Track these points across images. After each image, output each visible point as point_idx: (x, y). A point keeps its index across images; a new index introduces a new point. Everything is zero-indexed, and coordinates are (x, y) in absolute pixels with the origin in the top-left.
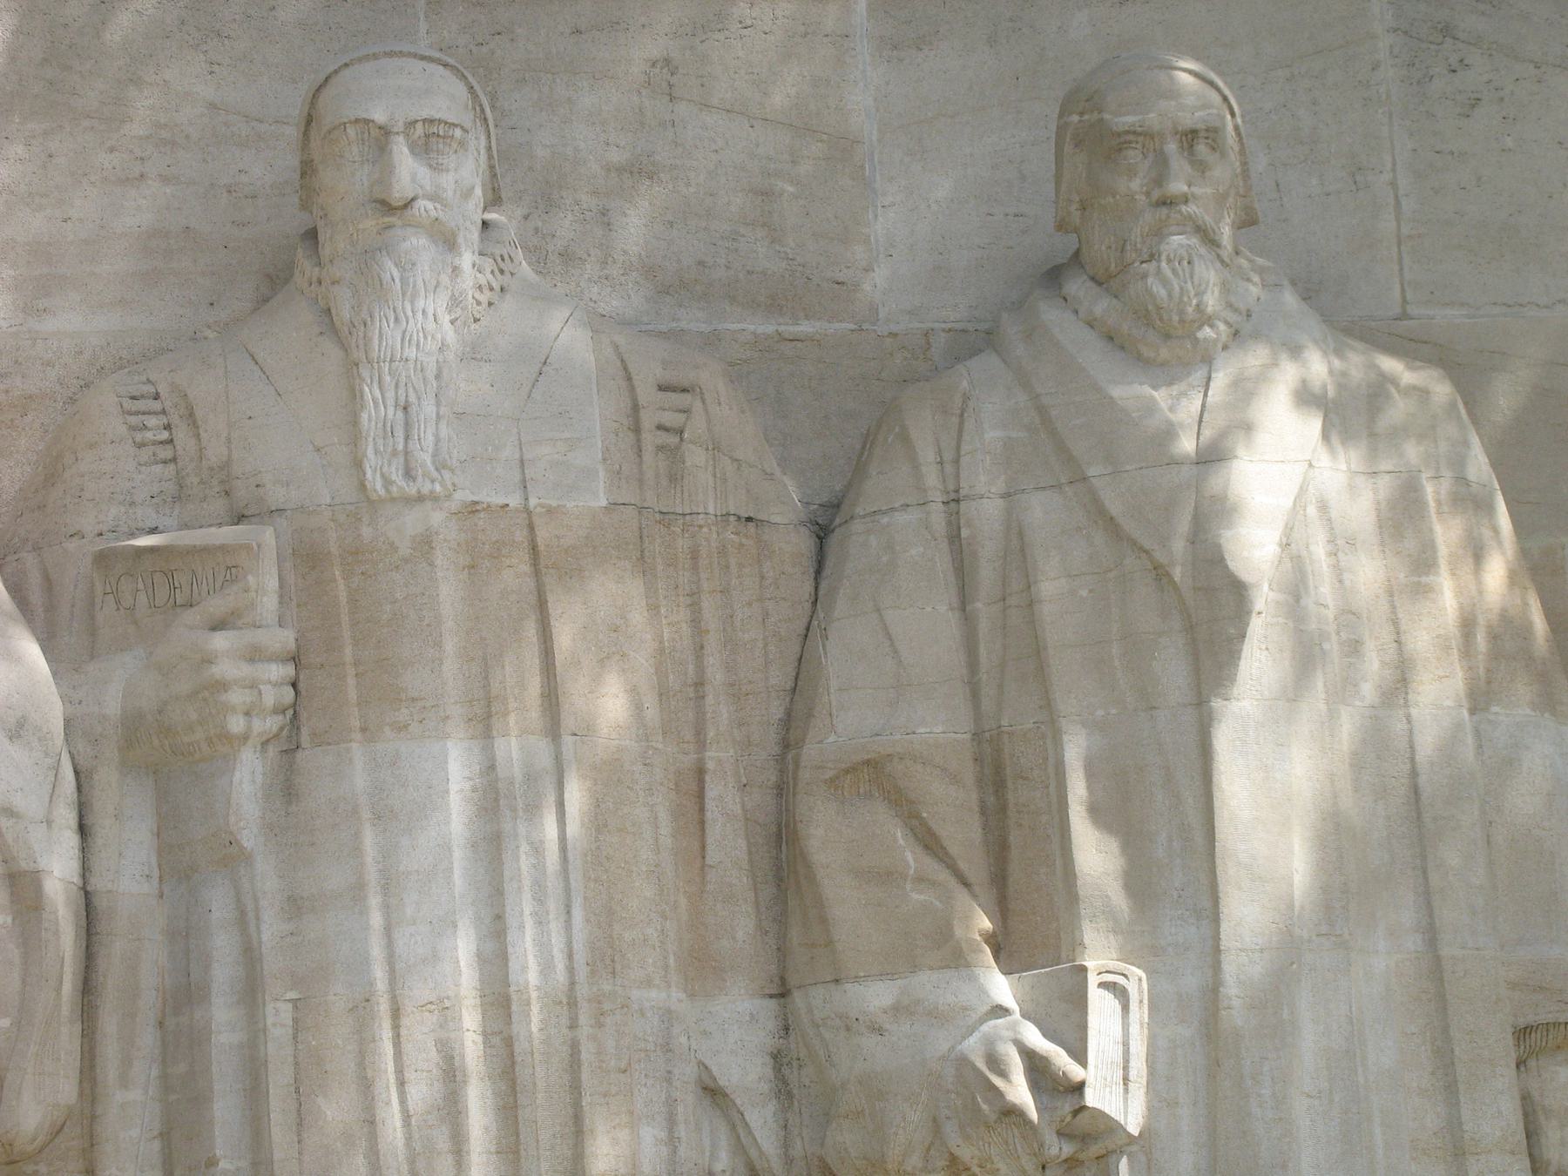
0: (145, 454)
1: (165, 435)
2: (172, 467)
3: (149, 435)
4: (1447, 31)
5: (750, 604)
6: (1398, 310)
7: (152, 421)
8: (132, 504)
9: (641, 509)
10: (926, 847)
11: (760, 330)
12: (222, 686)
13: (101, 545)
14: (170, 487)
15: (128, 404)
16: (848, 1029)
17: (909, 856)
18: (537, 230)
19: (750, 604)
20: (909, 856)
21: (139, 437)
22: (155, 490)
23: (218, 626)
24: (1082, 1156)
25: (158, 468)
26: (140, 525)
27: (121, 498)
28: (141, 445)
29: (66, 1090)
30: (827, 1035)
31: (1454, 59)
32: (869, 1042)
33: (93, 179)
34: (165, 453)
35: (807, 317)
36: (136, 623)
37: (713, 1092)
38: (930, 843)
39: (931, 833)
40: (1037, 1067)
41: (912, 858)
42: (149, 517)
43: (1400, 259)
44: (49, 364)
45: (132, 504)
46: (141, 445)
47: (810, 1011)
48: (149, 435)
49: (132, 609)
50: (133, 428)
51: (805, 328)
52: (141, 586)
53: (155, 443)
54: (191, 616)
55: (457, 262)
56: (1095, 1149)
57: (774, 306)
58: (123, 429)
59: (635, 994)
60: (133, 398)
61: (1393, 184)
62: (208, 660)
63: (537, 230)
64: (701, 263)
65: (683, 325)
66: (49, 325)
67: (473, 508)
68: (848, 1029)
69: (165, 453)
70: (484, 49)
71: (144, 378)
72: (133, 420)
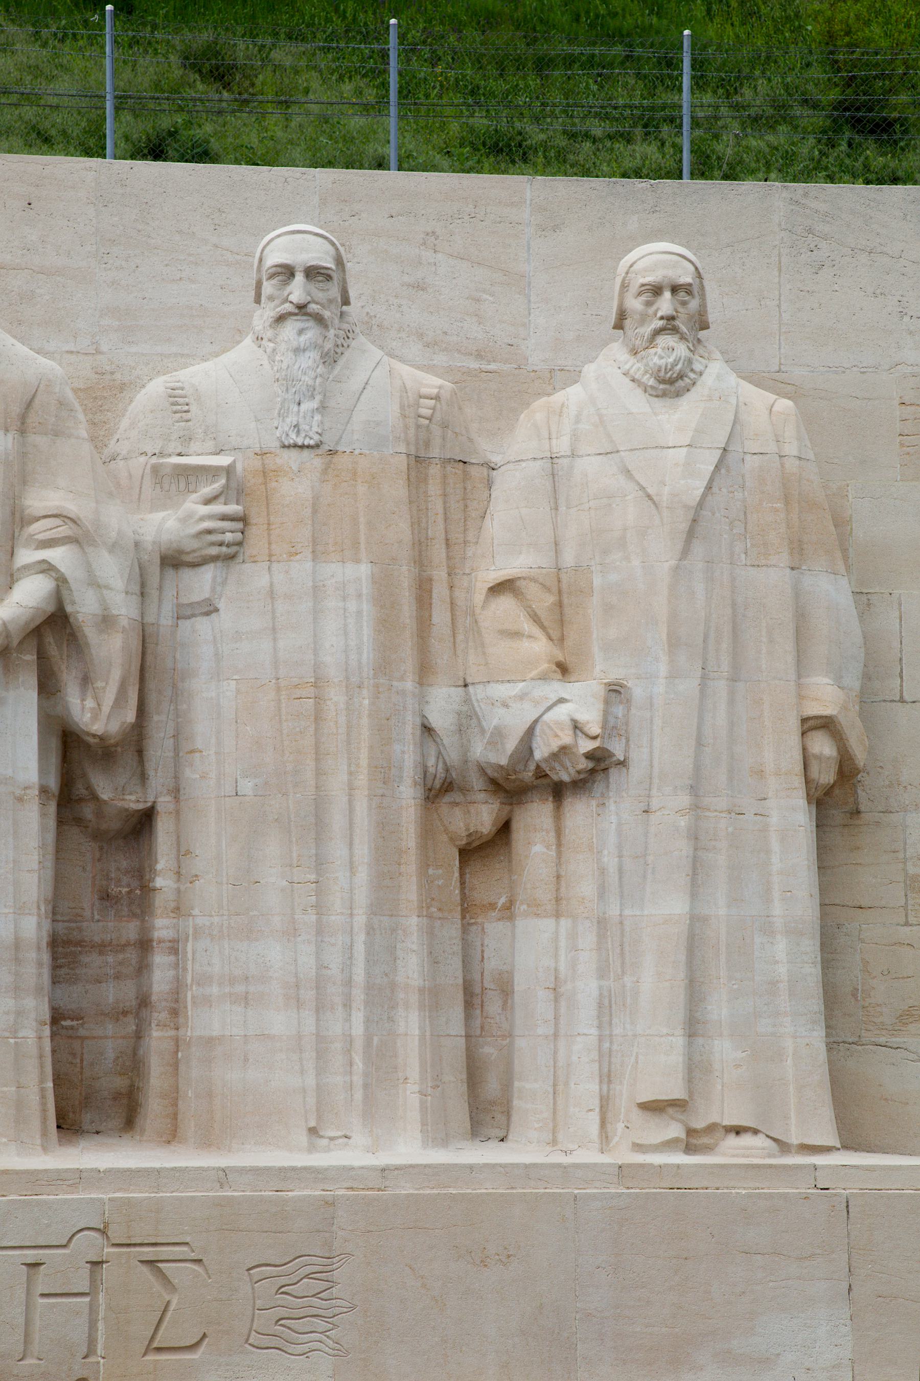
4: (810, 231)
5: (458, 502)
6: (777, 368)
9: (408, 455)
10: (534, 621)
11: (472, 366)
13: (154, 460)
16: (493, 704)
17: (526, 626)
18: (368, 313)
19: (458, 502)
20: (526, 626)
22: (181, 434)
23: (208, 502)
24: (598, 768)
29: (130, 716)
30: (483, 707)
31: (812, 246)
32: (502, 711)
35: (494, 361)
37: (427, 729)
38: (536, 619)
39: (536, 614)
40: (576, 727)
41: (527, 626)
43: (780, 343)
46: (175, 412)
47: (476, 695)
51: (492, 367)
54: (194, 496)
55: (327, 334)
56: (603, 766)
57: (479, 356)
59: (395, 683)
61: (779, 306)
63: (368, 313)
64: (445, 333)
65: (435, 362)
67: (332, 453)
68: (493, 704)
70: (347, 223)
72: (172, 399)
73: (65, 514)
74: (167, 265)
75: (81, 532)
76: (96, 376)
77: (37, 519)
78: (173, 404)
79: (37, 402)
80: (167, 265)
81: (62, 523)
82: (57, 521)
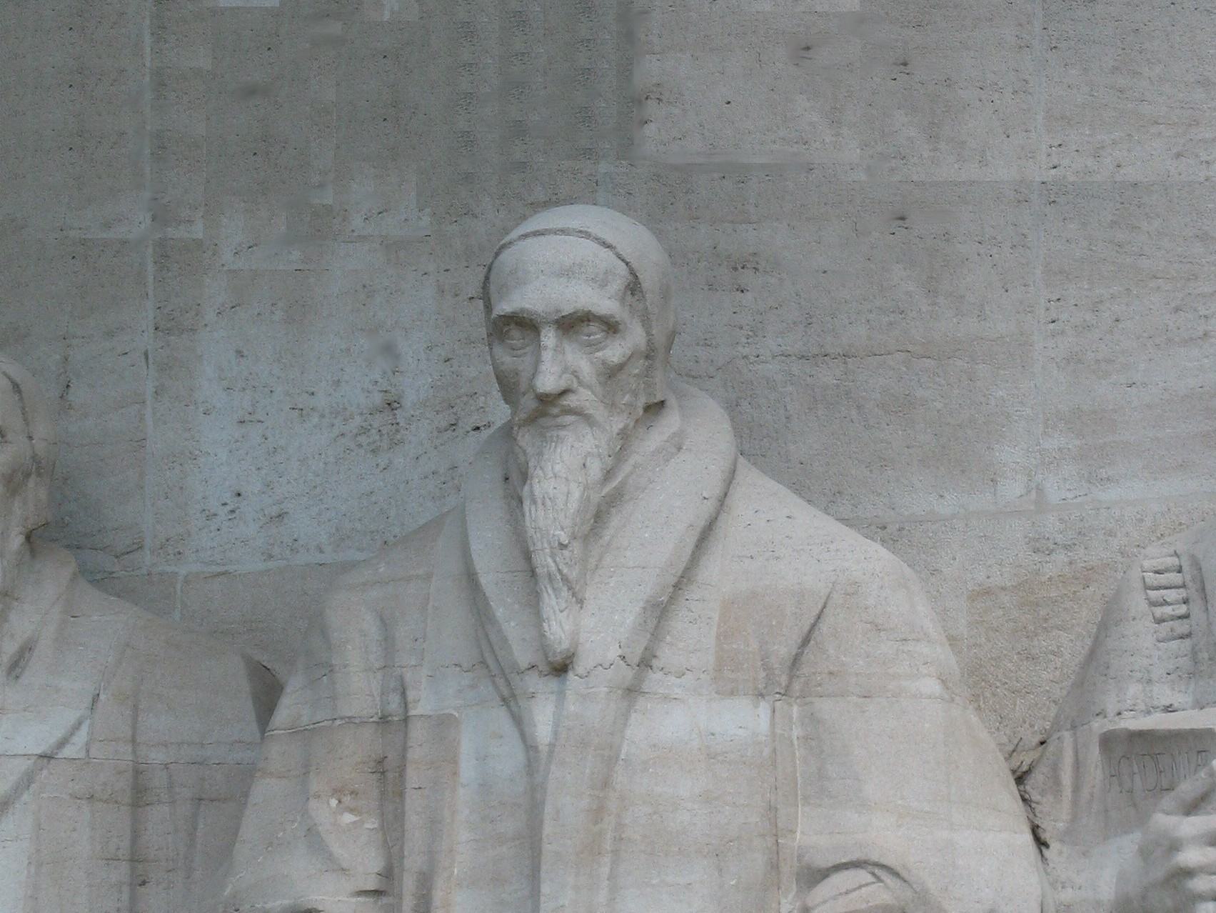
0: (1164, 628)
1: (1183, 609)
2: (1188, 642)
3: (1168, 610)
7: (1171, 595)
8: (1149, 681)
12: (1188, 873)
14: (1185, 662)
15: (1150, 577)
21: (1159, 611)
25: (1174, 644)
26: (1156, 703)
27: (1139, 675)
28: (1160, 621)
33: (1157, 341)
34: (1182, 627)
36: (1135, 805)
42: (1165, 694)
44: (1111, 534)
45: (1149, 681)
46: (1160, 621)
48: (1168, 610)
49: (1131, 791)
50: (1154, 604)
52: (1136, 770)
53: (1173, 618)
54: (1168, 801)
58: (1144, 606)
60: (1157, 572)
62: (1175, 846)
66: (1110, 494)
69: (1182, 627)
71: (1171, 551)
72: (1153, 594)
73: (875, 857)
74: (1177, 310)
75: (909, 894)
76: (1036, 558)
77: (825, 874)
78: (1154, 604)
79: (824, 627)
80: (1177, 310)
81: (870, 878)
82: (863, 876)
